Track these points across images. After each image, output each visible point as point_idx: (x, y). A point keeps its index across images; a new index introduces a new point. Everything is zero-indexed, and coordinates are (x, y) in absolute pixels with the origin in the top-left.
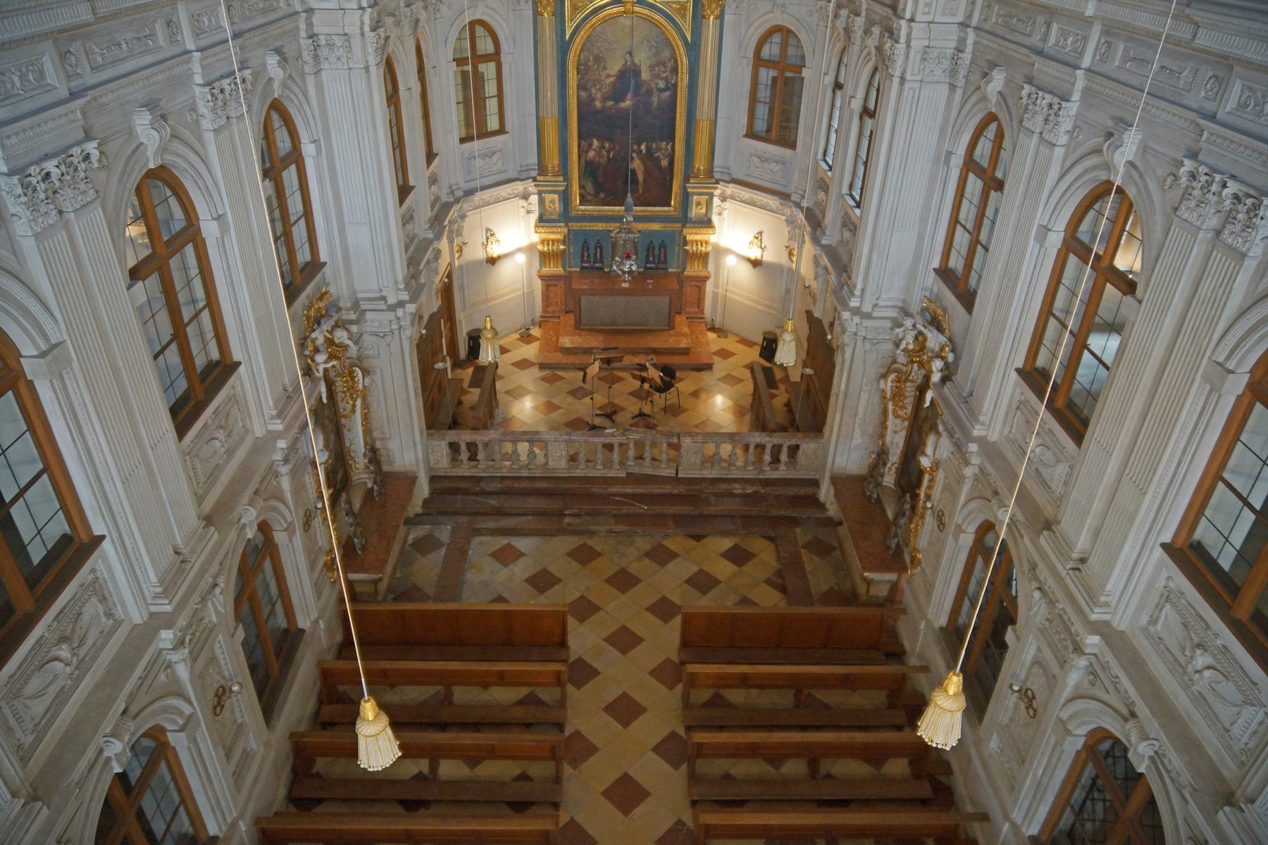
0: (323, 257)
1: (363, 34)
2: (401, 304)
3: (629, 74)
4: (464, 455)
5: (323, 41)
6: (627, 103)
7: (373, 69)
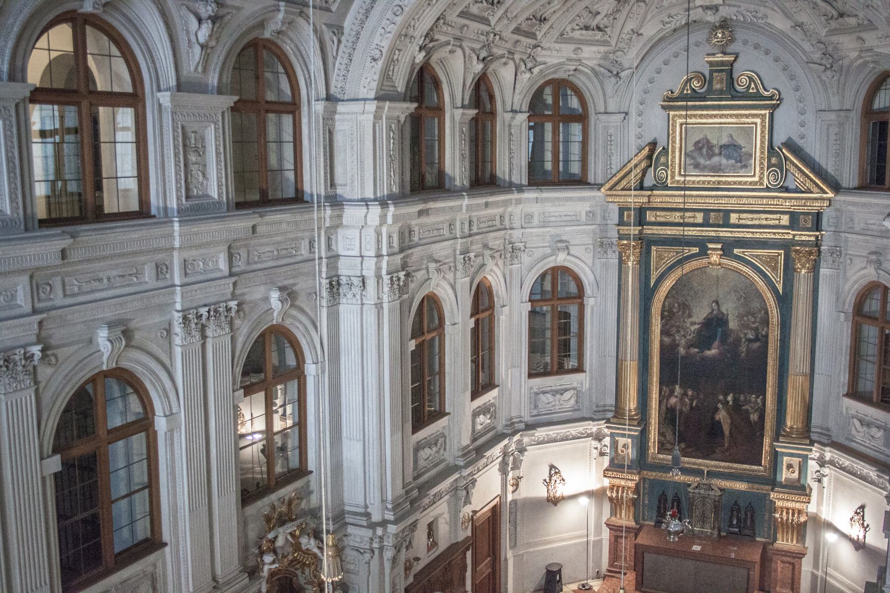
0: (311, 465)
1: (379, 277)
2: (384, 523)
3: (715, 324)
5: (344, 280)
6: (713, 352)
7: (386, 306)
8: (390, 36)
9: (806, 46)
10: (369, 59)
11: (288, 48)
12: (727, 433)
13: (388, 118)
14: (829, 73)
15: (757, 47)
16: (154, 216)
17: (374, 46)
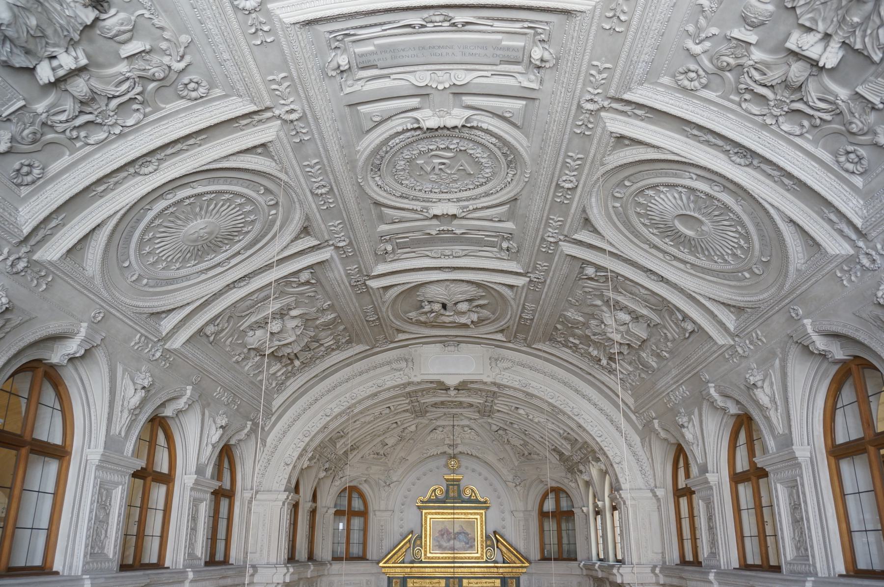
8: (300, 450)
9: (505, 472)
10: (283, 464)
11: (237, 453)
13: (289, 504)
14: (518, 488)
15: (473, 471)
16: (168, 568)
17: (287, 455)
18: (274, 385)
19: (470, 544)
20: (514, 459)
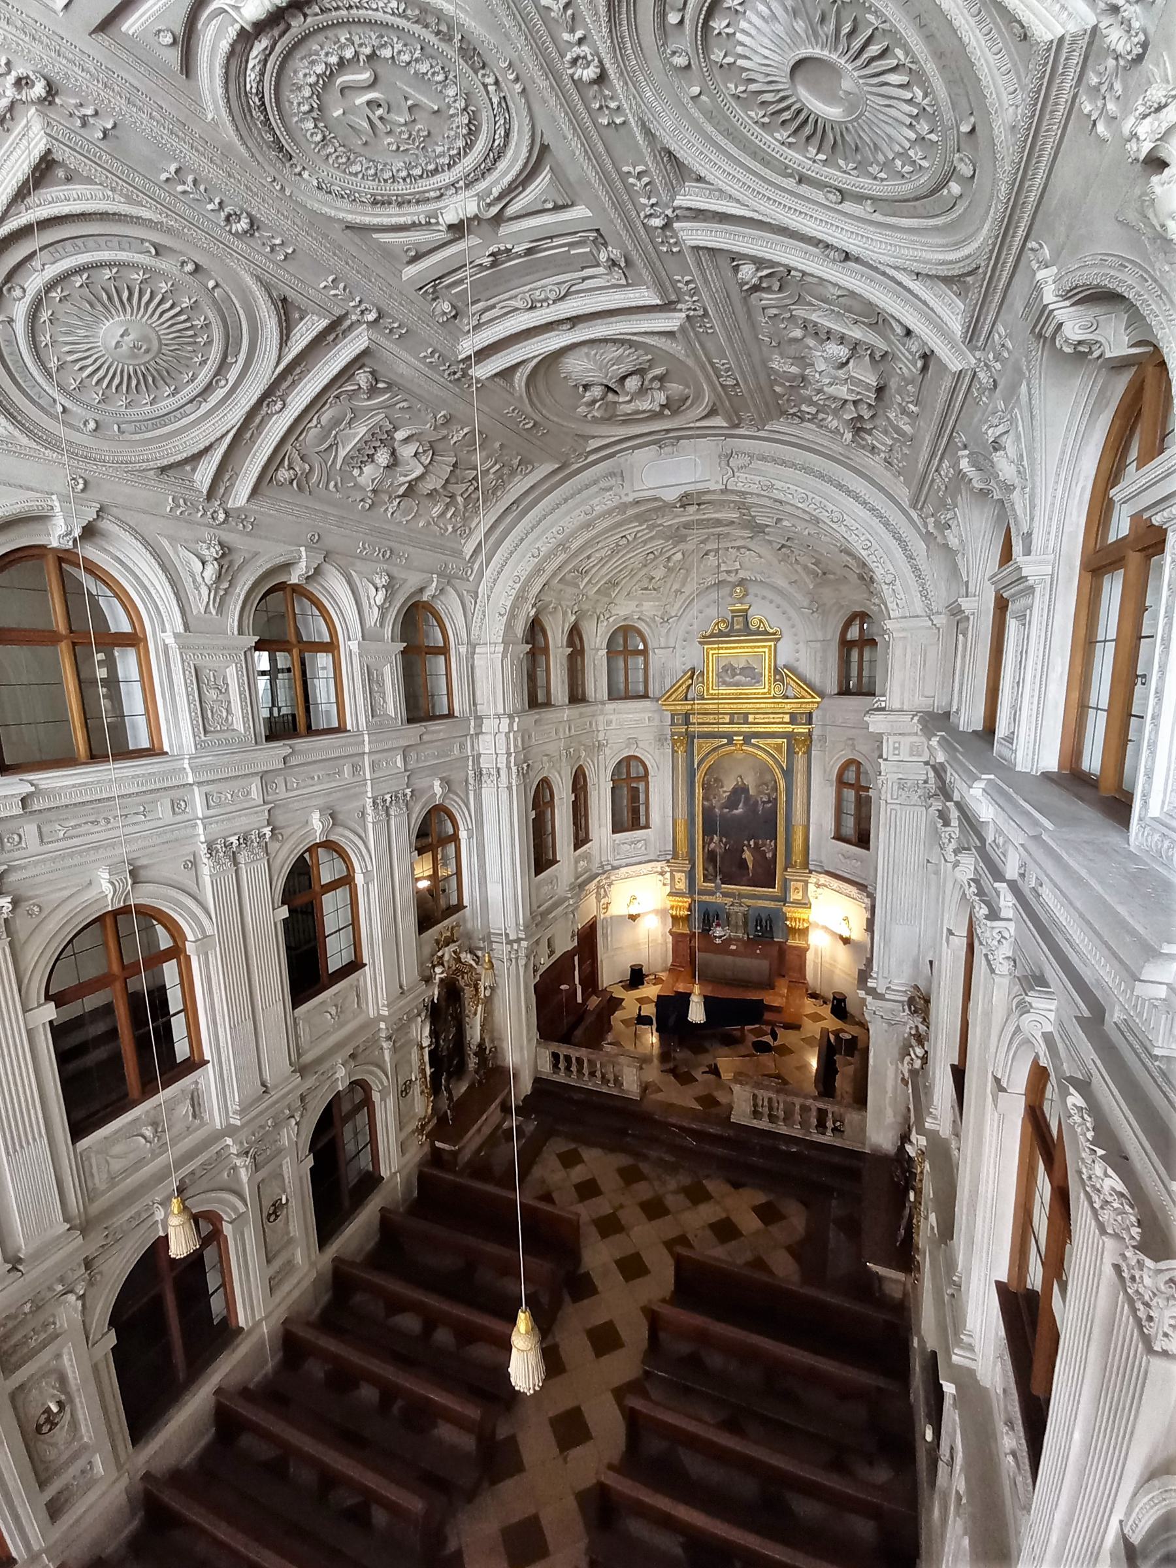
0: (466, 902)
1: (509, 768)
2: (518, 940)
3: (740, 791)
4: (562, 1065)
5: (484, 772)
6: (740, 811)
7: (514, 788)
9: (799, 596)
11: (439, 606)
12: (750, 866)
15: (764, 598)
18: (450, 529)
19: (756, 678)
20: (807, 580)
